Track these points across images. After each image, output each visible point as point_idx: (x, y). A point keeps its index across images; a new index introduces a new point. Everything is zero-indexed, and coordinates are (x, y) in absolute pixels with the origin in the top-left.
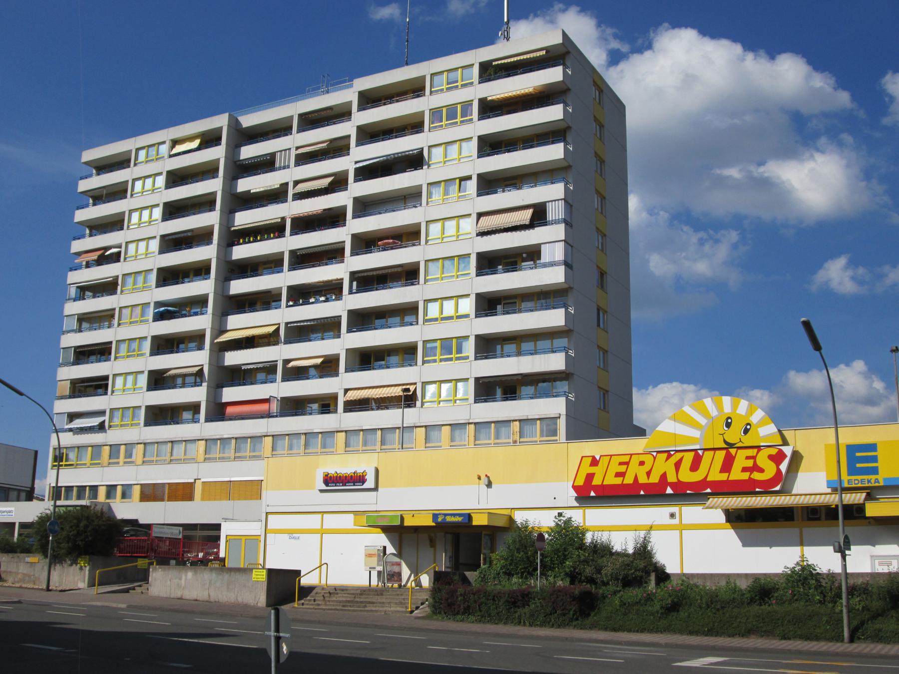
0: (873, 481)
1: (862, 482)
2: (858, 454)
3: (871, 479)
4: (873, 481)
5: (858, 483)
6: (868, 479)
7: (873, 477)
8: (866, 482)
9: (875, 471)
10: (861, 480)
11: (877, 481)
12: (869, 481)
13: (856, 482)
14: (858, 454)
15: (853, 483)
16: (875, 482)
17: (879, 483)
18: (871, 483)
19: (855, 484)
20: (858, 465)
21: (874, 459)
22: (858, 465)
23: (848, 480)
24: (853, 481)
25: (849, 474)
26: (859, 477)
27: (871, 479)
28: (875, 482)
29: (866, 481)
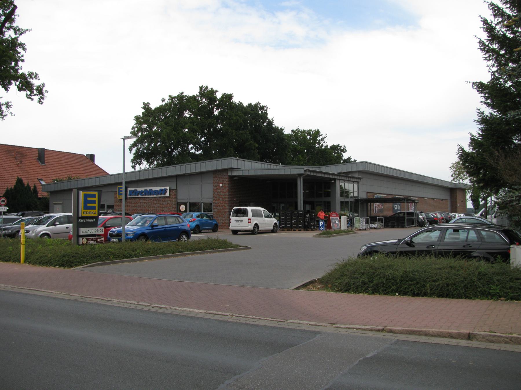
0: (94, 213)
3: (93, 212)
4: (94, 213)
12: (92, 213)
13: (87, 213)
19: (87, 214)
20: (89, 205)
22: (89, 205)
24: (86, 212)
26: (88, 211)
27: (93, 212)
28: (95, 213)
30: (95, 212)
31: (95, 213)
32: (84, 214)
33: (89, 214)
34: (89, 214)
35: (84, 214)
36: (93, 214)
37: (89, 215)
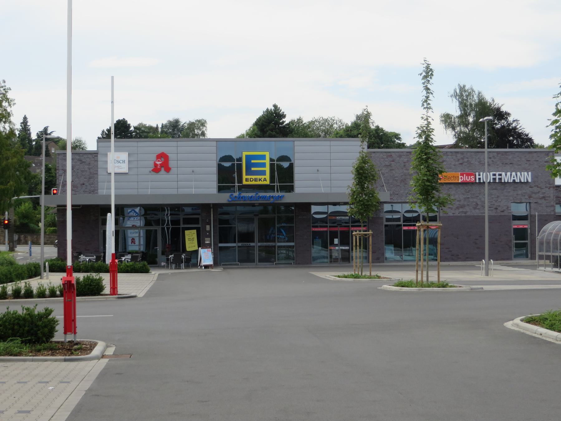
0: (262, 180)
3: (262, 178)
4: (262, 180)
6: (259, 178)
7: (263, 177)
8: (258, 180)
10: (255, 178)
12: (260, 180)
13: (252, 180)
15: (249, 180)
16: (264, 180)
17: (266, 181)
18: (262, 181)
19: (250, 181)
20: (253, 169)
22: (253, 169)
23: (246, 179)
25: (246, 175)
26: (254, 177)
27: (262, 178)
28: (264, 180)
29: (258, 179)
30: (264, 178)
31: (265, 180)
32: (246, 181)
33: (255, 181)
35: (246, 181)
36: (262, 181)
37: (254, 183)
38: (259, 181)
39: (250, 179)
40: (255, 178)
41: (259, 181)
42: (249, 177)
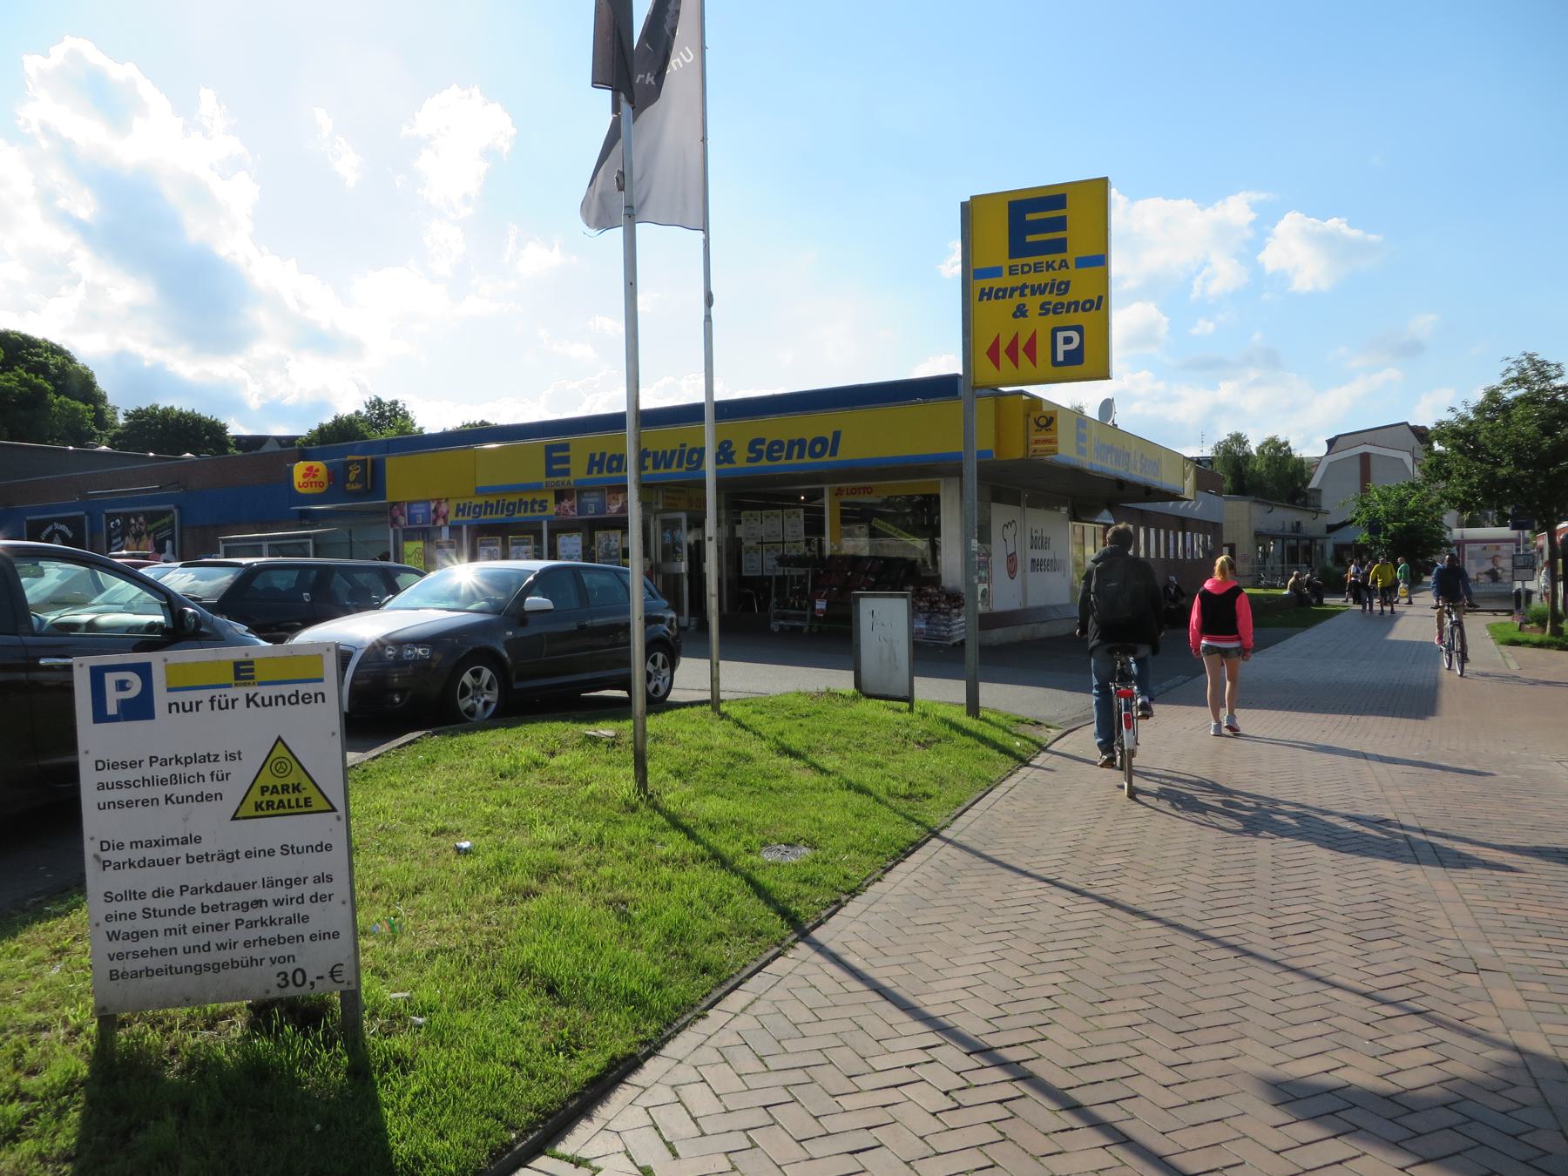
0: (1056, 265)
1: (1035, 267)
2: (1030, 217)
3: (1054, 262)
4: (1056, 265)
5: (1028, 272)
7: (1056, 258)
9: (1060, 246)
10: (1035, 264)
11: (1064, 264)
12: (1050, 266)
13: (1026, 269)
14: (1030, 217)
15: (1020, 271)
18: (1054, 269)
19: (1023, 272)
20: (1030, 239)
21: (1061, 224)
22: (1030, 239)
23: (1010, 267)
26: (1031, 260)
27: (1054, 262)
30: (1062, 261)
32: (1010, 274)
33: (1035, 271)
34: (1035, 271)
36: (1054, 269)
38: (1047, 270)
39: (1023, 266)
40: (1035, 264)
41: (1047, 270)
42: (1019, 261)
